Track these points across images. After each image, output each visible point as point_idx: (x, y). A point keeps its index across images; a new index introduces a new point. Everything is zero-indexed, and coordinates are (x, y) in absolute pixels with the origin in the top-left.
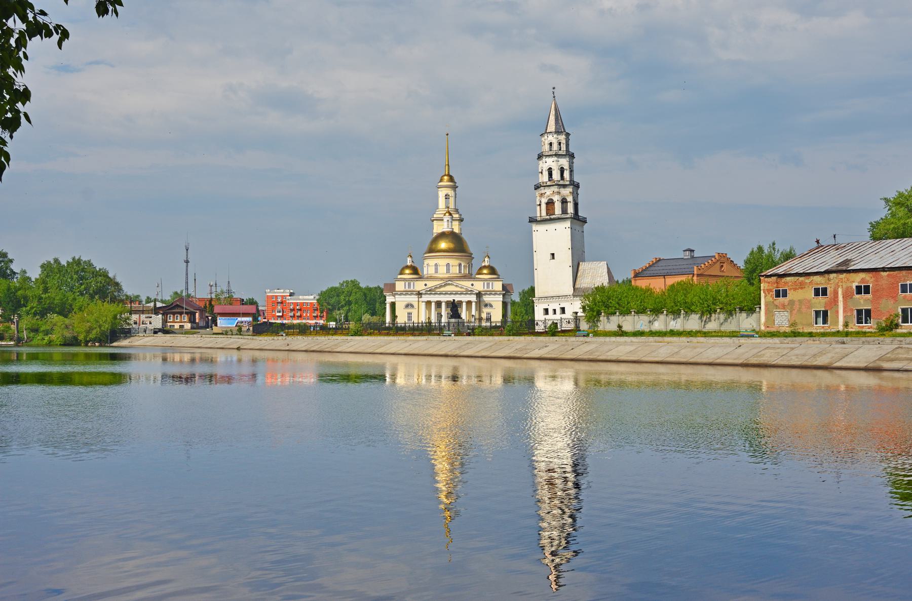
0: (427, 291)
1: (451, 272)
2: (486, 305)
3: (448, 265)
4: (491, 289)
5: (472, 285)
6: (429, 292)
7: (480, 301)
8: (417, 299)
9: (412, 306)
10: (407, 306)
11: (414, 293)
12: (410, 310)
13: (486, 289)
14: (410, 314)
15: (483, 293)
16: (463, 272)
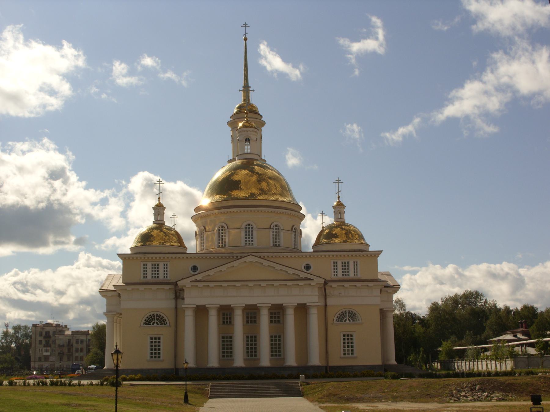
0: (197, 281)
1: (255, 243)
2: (341, 317)
3: (249, 227)
4: (352, 275)
5: (308, 267)
6: (200, 285)
7: (326, 305)
8: (173, 302)
9: (161, 320)
10: (149, 321)
11: (167, 287)
12: (155, 330)
13: (340, 275)
14: (155, 341)
15: (334, 285)
16: (282, 243)
